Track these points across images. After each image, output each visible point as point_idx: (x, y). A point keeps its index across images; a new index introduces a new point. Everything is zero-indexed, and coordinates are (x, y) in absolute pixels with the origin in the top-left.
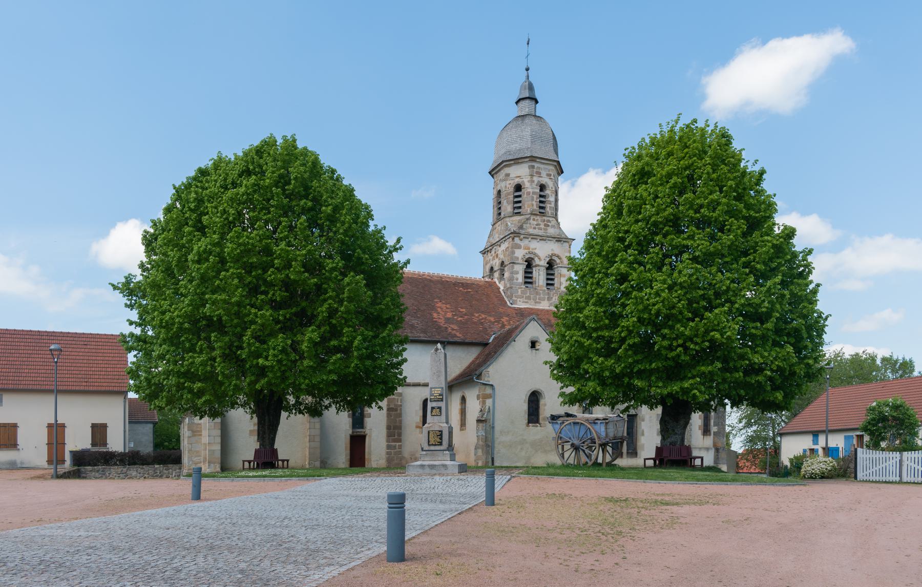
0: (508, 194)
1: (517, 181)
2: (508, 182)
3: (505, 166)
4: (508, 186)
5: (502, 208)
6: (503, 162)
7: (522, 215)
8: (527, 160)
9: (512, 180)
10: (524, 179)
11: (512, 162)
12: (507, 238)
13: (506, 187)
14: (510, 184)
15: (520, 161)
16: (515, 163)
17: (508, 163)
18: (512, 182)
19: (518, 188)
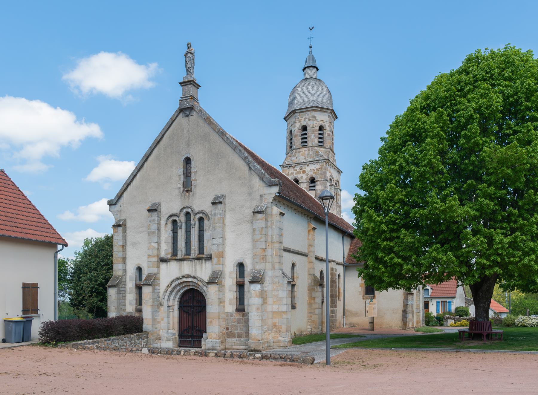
0: (316, 131)
1: (321, 123)
2: (315, 122)
3: (313, 110)
4: (315, 125)
5: (309, 140)
6: (314, 107)
7: (325, 148)
8: (329, 111)
9: (318, 121)
10: (325, 124)
11: (319, 109)
12: (320, 161)
13: (313, 125)
14: (316, 124)
15: (324, 110)
16: (321, 111)
17: (316, 109)
18: (318, 123)
19: (321, 128)
